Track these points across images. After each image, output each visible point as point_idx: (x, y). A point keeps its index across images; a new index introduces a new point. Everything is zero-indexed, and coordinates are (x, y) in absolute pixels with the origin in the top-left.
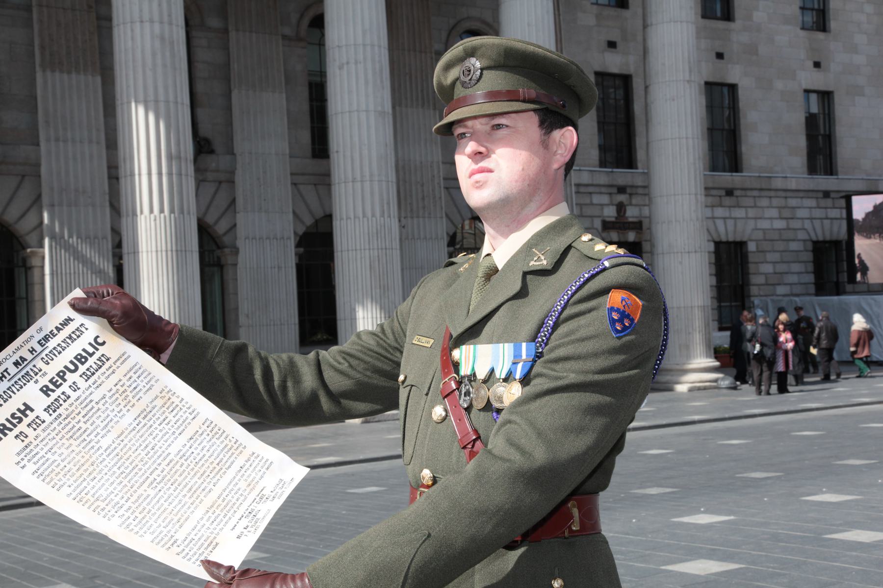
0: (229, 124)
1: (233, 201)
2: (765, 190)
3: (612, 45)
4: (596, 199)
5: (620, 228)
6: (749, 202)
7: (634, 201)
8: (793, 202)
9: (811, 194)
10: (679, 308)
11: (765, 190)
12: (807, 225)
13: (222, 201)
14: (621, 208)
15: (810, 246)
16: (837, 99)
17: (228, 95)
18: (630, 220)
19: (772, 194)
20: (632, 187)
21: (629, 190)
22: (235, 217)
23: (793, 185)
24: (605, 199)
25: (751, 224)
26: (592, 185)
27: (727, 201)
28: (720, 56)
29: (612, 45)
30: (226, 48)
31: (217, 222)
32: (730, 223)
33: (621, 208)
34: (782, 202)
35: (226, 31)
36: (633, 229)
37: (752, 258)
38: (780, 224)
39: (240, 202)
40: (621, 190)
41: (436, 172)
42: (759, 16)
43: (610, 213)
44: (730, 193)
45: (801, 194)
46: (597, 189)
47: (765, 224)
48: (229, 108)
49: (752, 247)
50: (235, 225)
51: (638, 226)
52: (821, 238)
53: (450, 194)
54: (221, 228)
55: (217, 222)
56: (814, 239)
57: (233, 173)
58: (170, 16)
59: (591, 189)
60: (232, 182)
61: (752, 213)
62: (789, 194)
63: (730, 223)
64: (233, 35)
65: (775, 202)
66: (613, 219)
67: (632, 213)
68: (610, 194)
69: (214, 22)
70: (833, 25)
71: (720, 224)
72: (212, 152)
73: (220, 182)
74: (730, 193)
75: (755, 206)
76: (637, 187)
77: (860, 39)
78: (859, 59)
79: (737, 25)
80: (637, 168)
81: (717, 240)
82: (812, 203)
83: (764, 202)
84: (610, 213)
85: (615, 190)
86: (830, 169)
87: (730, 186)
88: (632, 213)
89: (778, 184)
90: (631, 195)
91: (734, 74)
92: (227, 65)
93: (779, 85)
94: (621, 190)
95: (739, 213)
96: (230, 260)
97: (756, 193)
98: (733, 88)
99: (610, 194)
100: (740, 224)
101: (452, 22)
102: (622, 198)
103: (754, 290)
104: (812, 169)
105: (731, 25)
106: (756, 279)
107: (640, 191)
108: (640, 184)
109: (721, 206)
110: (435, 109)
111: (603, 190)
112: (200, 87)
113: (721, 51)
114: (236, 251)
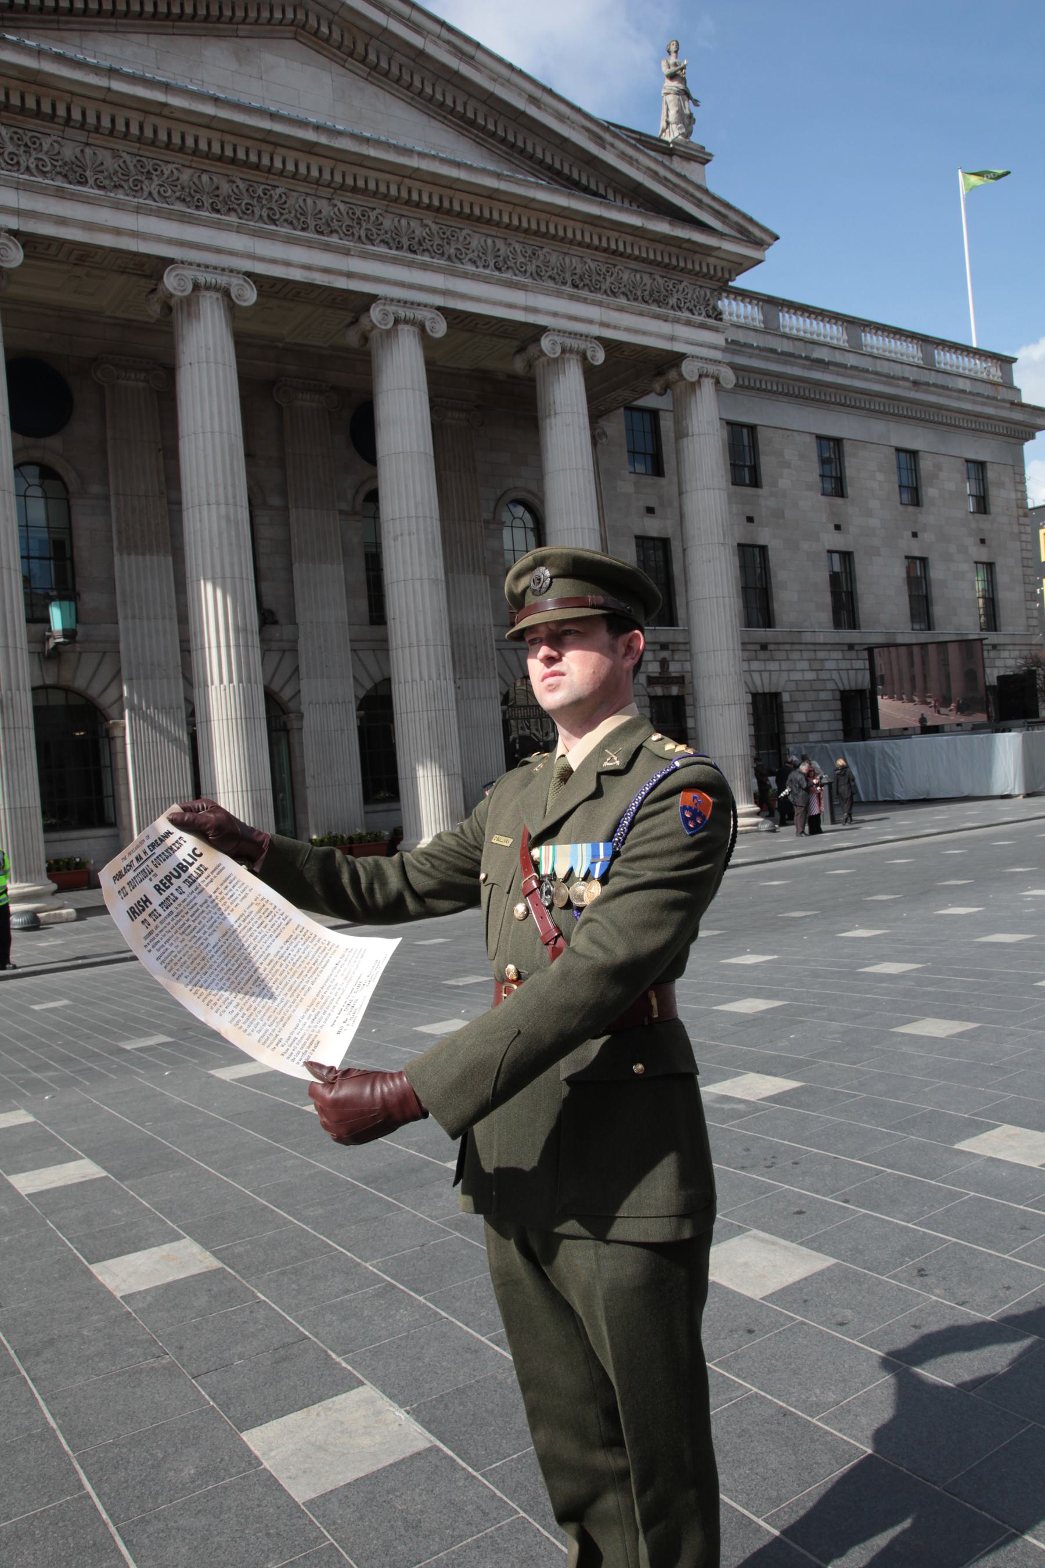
0: (291, 595)
1: (297, 669)
3: (650, 510)
5: (664, 683)
6: (781, 655)
7: (676, 657)
8: (821, 655)
9: (837, 647)
10: (721, 757)
11: (796, 643)
12: (835, 675)
14: (664, 664)
15: (838, 695)
16: (857, 558)
17: (290, 569)
18: (673, 675)
19: (803, 647)
21: (671, 647)
22: (299, 684)
23: (821, 639)
25: (785, 675)
27: (762, 655)
28: (750, 520)
29: (650, 510)
30: (287, 524)
31: (282, 689)
32: (766, 675)
34: (811, 655)
35: (286, 508)
36: (675, 683)
37: (785, 709)
38: (810, 676)
39: (303, 669)
40: (664, 647)
41: (488, 635)
42: (784, 483)
44: (764, 647)
45: (829, 647)
47: (797, 676)
48: (291, 581)
49: (786, 697)
50: (299, 691)
51: (680, 680)
52: (847, 688)
53: (502, 654)
54: (286, 694)
55: (282, 689)
56: (842, 688)
57: (296, 641)
58: (234, 497)
60: (294, 650)
61: (785, 665)
62: (818, 647)
63: (766, 675)
64: (293, 512)
65: (806, 655)
67: (674, 668)
68: (654, 651)
69: (275, 501)
70: (849, 491)
72: (275, 622)
73: (284, 651)
74: (764, 647)
75: (788, 659)
77: (874, 504)
78: (874, 522)
79: (764, 491)
80: (677, 626)
81: (754, 691)
82: (838, 655)
83: (795, 655)
85: (658, 647)
86: (854, 625)
87: (764, 641)
88: (674, 668)
89: (807, 638)
90: (673, 651)
91: (763, 536)
92: (289, 539)
93: (805, 546)
94: (664, 647)
95: (773, 666)
96: (295, 724)
97: (788, 647)
98: (763, 549)
99: (654, 651)
100: (774, 676)
101: (499, 492)
103: (789, 738)
104: (837, 624)
105: (759, 491)
106: (791, 728)
107: (682, 647)
108: (681, 640)
109: (757, 659)
110: (485, 574)
112: (263, 563)
113: (750, 515)
114: (301, 716)
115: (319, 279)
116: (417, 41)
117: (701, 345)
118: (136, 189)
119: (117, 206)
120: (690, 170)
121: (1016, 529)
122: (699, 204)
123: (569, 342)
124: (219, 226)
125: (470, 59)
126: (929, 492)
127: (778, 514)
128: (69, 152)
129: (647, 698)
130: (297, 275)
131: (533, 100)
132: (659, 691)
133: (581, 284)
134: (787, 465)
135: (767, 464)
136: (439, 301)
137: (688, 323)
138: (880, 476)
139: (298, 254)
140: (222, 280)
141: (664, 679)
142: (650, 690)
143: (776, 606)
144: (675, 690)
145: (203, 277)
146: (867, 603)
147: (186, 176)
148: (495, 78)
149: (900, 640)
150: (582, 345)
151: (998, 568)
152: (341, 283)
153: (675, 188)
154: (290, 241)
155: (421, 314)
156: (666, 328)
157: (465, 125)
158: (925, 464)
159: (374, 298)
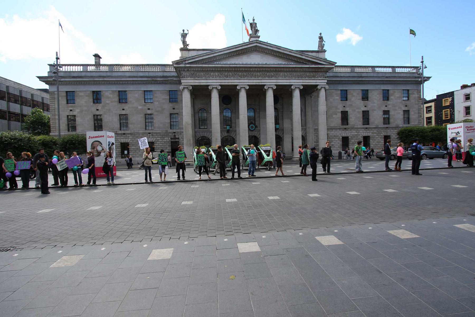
2: (353, 128)
11: (353, 128)
13: (259, 133)
28: (344, 107)
42: (353, 99)
49: (350, 137)
70: (369, 99)
71: (343, 134)
74: (345, 129)
78: (375, 105)
89: (356, 127)
91: (347, 109)
93: (357, 110)
106: (350, 143)
115: (257, 84)
116: (272, 48)
118: (234, 77)
119: (231, 79)
120: (320, 55)
121: (417, 103)
122: (321, 61)
123: (296, 86)
124: (244, 79)
125: (280, 49)
126: (391, 97)
127: (351, 105)
128: (226, 74)
130: (254, 84)
131: (290, 52)
133: (299, 77)
134: (354, 96)
135: (349, 97)
136: (275, 84)
137: (319, 80)
138: (378, 96)
139: (255, 81)
140: (244, 86)
143: (349, 121)
145: (242, 86)
146: (372, 119)
147: (240, 74)
148: (284, 50)
149: (379, 126)
150: (298, 86)
151: (410, 111)
152: (261, 84)
153: (316, 59)
154: (253, 79)
155: (271, 86)
156: (315, 81)
157: (280, 57)
158: (390, 92)
159: (265, 85)
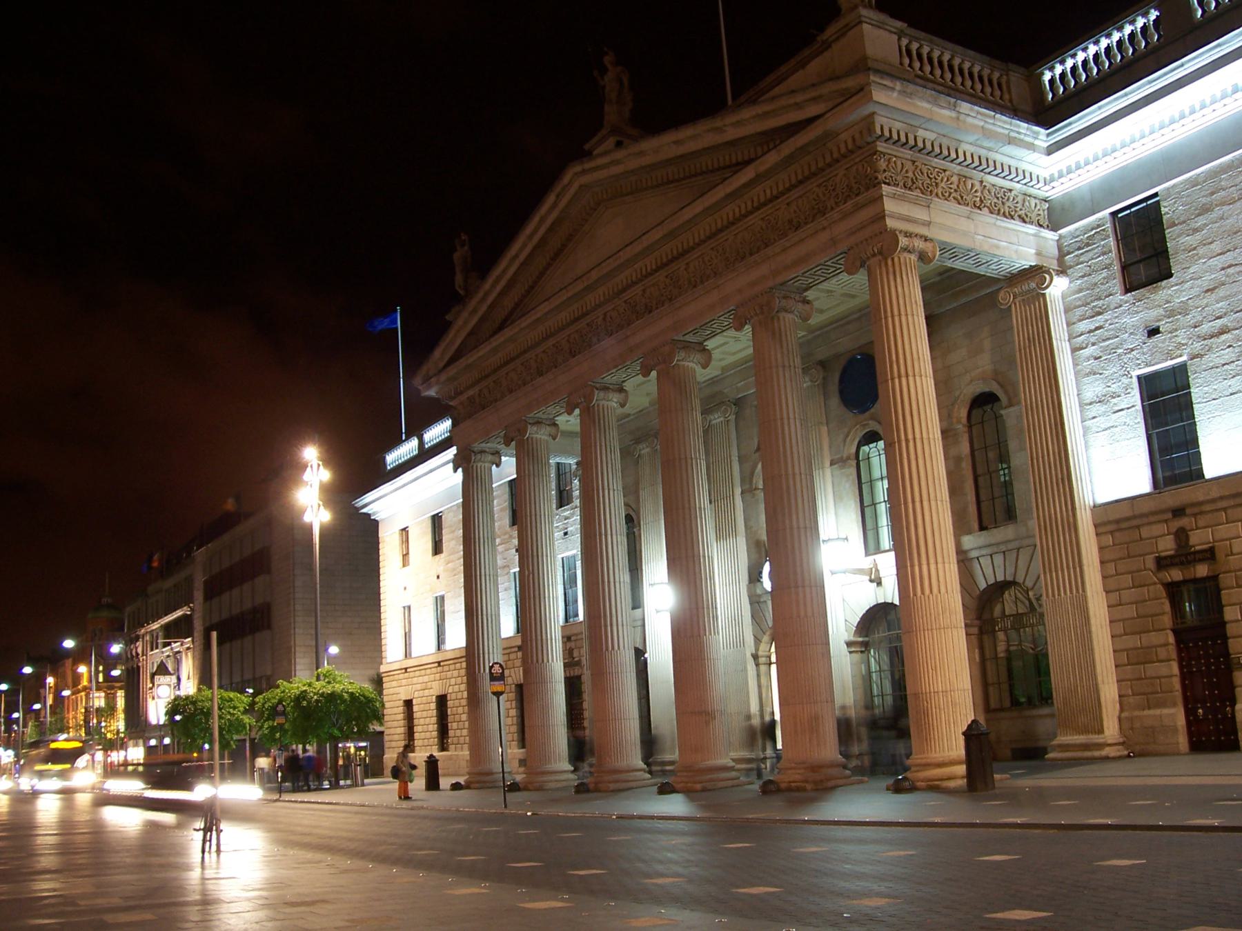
4: (1145, 532)
5: (1182, 563)
7: (1201, 523)
14: (1181, 536)
18: (1198, 548)
20: (1193, 505)
21: (1188, 511)
24: (1160, 529)
26: (1134, 517)
33: (1181, 536)
36: (1201, 560)
40: (1178, 512)
43: (1167, 545)
46: (1145, 520)
51: (1209, 555)
59: (1135, 522)
66: (1172, 553)
67: (1199, 539)
68: (1166, 521)
76: (1201, 503)
84: (1167, 545)
85: (1170, 515)
99: (1166, 521)
102: (1184, 522)
107: (1207, 508)
111: (1152, 519)
117: (863, 227)
129: (1159, 587)
132: (1176, 575)
137: (845, 216)
141: (1184, 555)
142: (1161, 575)
144: (1202, 570)
